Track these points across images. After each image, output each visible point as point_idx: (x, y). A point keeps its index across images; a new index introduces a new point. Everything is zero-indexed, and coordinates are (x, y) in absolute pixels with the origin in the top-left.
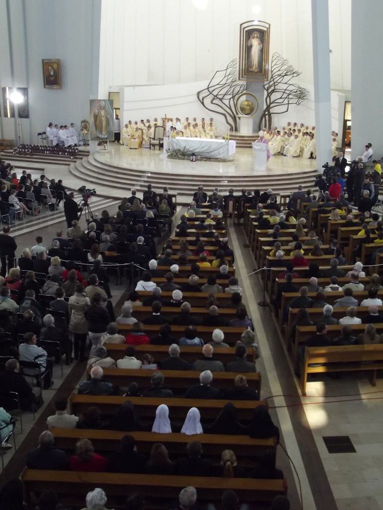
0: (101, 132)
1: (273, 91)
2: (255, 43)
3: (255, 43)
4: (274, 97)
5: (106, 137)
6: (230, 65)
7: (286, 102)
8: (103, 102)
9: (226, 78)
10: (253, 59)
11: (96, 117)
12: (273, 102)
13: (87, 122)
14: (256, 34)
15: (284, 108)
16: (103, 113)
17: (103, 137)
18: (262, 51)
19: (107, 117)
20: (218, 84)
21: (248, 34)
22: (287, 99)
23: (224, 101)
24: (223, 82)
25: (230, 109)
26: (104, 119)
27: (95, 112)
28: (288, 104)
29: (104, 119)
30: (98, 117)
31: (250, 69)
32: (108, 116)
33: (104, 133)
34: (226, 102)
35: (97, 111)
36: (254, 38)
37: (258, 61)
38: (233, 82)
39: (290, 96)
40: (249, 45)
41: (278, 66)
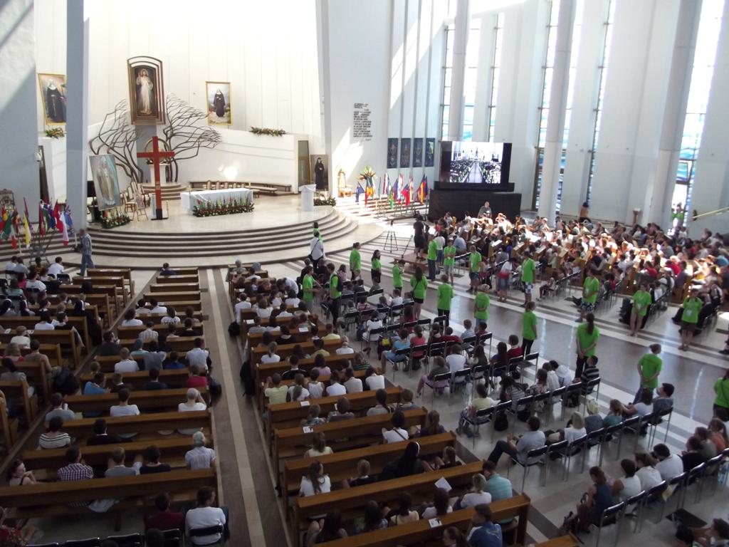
0: (108, 199)
1: (171, 136)
2: (145, 82)
3: (145, 82)
4: (174, 142)
5: (114, 203)
6: (119, 106)
7: (197, 145)
8: (104, 157)
9: (117, 122)
10: (144, 99)
11: (100, 178)
12: (177, 147)
13: (11, 192)
14: (145, 72)
15: (193, 152)
16: (106, 172)
17: (111, 204)
18: (154, 91)
19: (110, 177)
20: (111, 130)
21: (135, 72)
22: (197, 143)
23: (115, 149)
24: (116, 127)
25: (126, 158)
26: (108, 180)
27: (97, 172)
28: (199, 147)
29: (108, 180)
30: (102, 179)
31: (142, 112)
32: (112, 176)
33: (111, 199)
34: (120, 150)
35: (99, 170)
36: (142, 76)
37: (150, 102)
38: (124, 127)
39: (201, 140)
40: (138, 84)
41: (174, 108)
